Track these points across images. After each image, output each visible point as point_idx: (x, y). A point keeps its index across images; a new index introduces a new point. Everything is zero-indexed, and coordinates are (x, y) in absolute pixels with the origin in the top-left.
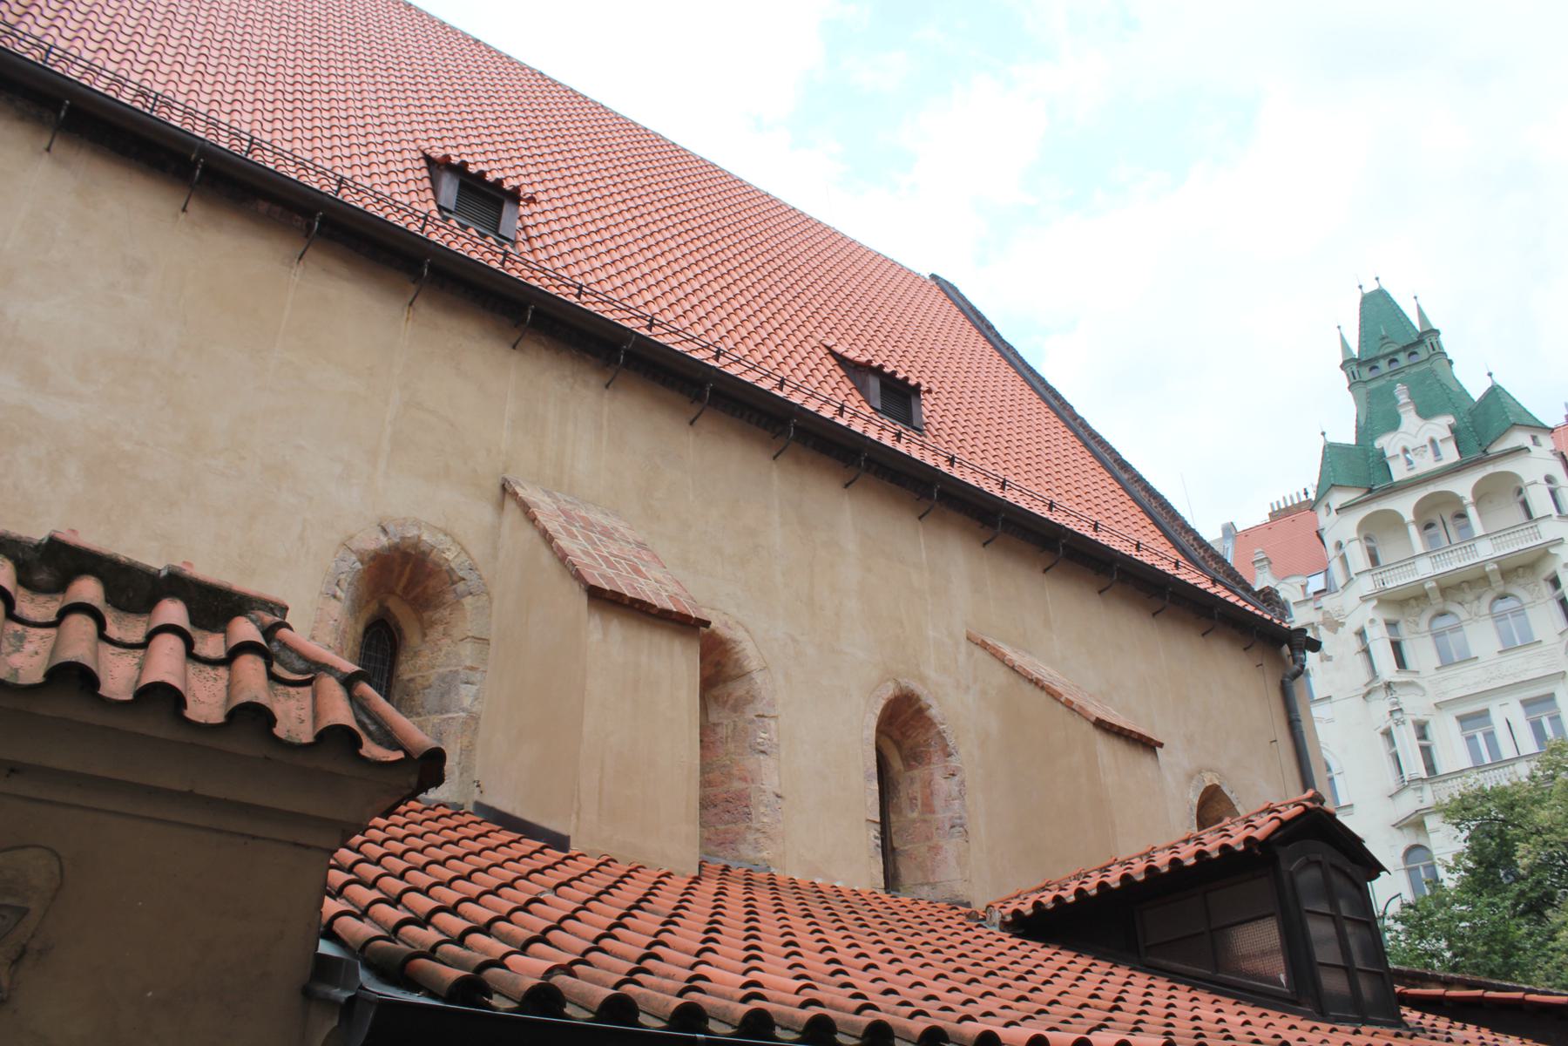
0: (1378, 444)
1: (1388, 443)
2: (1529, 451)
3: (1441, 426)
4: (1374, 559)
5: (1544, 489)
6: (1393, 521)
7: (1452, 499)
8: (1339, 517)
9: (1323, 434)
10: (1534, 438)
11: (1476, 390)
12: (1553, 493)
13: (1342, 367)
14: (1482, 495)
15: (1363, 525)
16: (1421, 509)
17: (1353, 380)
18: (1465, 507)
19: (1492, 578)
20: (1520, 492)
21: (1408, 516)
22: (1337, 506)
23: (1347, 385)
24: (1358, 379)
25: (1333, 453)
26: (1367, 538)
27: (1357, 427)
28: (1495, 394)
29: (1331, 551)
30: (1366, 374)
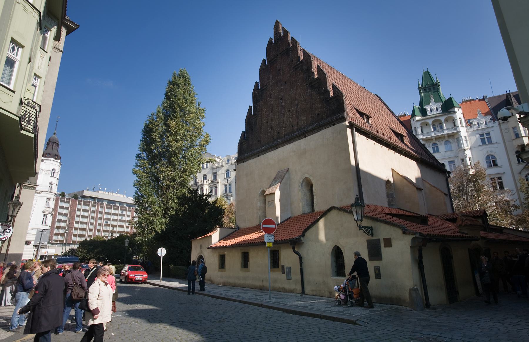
1: (428, 108)
2: (457, 112)
3: (439, 105)
4: (422, 132)
5: (459, 120)
6: (427, 125)
7: (440, 120)
10: (458, 109)
11: (447, 98)
12: (460, 121)
14: (446, 120)
15: (421, 124)
16: (433, 122)
18: (442, 123)
19: (446, 137)
20: (454, 120)
26: (421, 127)
27: (420, 102)
28: (450, 99)
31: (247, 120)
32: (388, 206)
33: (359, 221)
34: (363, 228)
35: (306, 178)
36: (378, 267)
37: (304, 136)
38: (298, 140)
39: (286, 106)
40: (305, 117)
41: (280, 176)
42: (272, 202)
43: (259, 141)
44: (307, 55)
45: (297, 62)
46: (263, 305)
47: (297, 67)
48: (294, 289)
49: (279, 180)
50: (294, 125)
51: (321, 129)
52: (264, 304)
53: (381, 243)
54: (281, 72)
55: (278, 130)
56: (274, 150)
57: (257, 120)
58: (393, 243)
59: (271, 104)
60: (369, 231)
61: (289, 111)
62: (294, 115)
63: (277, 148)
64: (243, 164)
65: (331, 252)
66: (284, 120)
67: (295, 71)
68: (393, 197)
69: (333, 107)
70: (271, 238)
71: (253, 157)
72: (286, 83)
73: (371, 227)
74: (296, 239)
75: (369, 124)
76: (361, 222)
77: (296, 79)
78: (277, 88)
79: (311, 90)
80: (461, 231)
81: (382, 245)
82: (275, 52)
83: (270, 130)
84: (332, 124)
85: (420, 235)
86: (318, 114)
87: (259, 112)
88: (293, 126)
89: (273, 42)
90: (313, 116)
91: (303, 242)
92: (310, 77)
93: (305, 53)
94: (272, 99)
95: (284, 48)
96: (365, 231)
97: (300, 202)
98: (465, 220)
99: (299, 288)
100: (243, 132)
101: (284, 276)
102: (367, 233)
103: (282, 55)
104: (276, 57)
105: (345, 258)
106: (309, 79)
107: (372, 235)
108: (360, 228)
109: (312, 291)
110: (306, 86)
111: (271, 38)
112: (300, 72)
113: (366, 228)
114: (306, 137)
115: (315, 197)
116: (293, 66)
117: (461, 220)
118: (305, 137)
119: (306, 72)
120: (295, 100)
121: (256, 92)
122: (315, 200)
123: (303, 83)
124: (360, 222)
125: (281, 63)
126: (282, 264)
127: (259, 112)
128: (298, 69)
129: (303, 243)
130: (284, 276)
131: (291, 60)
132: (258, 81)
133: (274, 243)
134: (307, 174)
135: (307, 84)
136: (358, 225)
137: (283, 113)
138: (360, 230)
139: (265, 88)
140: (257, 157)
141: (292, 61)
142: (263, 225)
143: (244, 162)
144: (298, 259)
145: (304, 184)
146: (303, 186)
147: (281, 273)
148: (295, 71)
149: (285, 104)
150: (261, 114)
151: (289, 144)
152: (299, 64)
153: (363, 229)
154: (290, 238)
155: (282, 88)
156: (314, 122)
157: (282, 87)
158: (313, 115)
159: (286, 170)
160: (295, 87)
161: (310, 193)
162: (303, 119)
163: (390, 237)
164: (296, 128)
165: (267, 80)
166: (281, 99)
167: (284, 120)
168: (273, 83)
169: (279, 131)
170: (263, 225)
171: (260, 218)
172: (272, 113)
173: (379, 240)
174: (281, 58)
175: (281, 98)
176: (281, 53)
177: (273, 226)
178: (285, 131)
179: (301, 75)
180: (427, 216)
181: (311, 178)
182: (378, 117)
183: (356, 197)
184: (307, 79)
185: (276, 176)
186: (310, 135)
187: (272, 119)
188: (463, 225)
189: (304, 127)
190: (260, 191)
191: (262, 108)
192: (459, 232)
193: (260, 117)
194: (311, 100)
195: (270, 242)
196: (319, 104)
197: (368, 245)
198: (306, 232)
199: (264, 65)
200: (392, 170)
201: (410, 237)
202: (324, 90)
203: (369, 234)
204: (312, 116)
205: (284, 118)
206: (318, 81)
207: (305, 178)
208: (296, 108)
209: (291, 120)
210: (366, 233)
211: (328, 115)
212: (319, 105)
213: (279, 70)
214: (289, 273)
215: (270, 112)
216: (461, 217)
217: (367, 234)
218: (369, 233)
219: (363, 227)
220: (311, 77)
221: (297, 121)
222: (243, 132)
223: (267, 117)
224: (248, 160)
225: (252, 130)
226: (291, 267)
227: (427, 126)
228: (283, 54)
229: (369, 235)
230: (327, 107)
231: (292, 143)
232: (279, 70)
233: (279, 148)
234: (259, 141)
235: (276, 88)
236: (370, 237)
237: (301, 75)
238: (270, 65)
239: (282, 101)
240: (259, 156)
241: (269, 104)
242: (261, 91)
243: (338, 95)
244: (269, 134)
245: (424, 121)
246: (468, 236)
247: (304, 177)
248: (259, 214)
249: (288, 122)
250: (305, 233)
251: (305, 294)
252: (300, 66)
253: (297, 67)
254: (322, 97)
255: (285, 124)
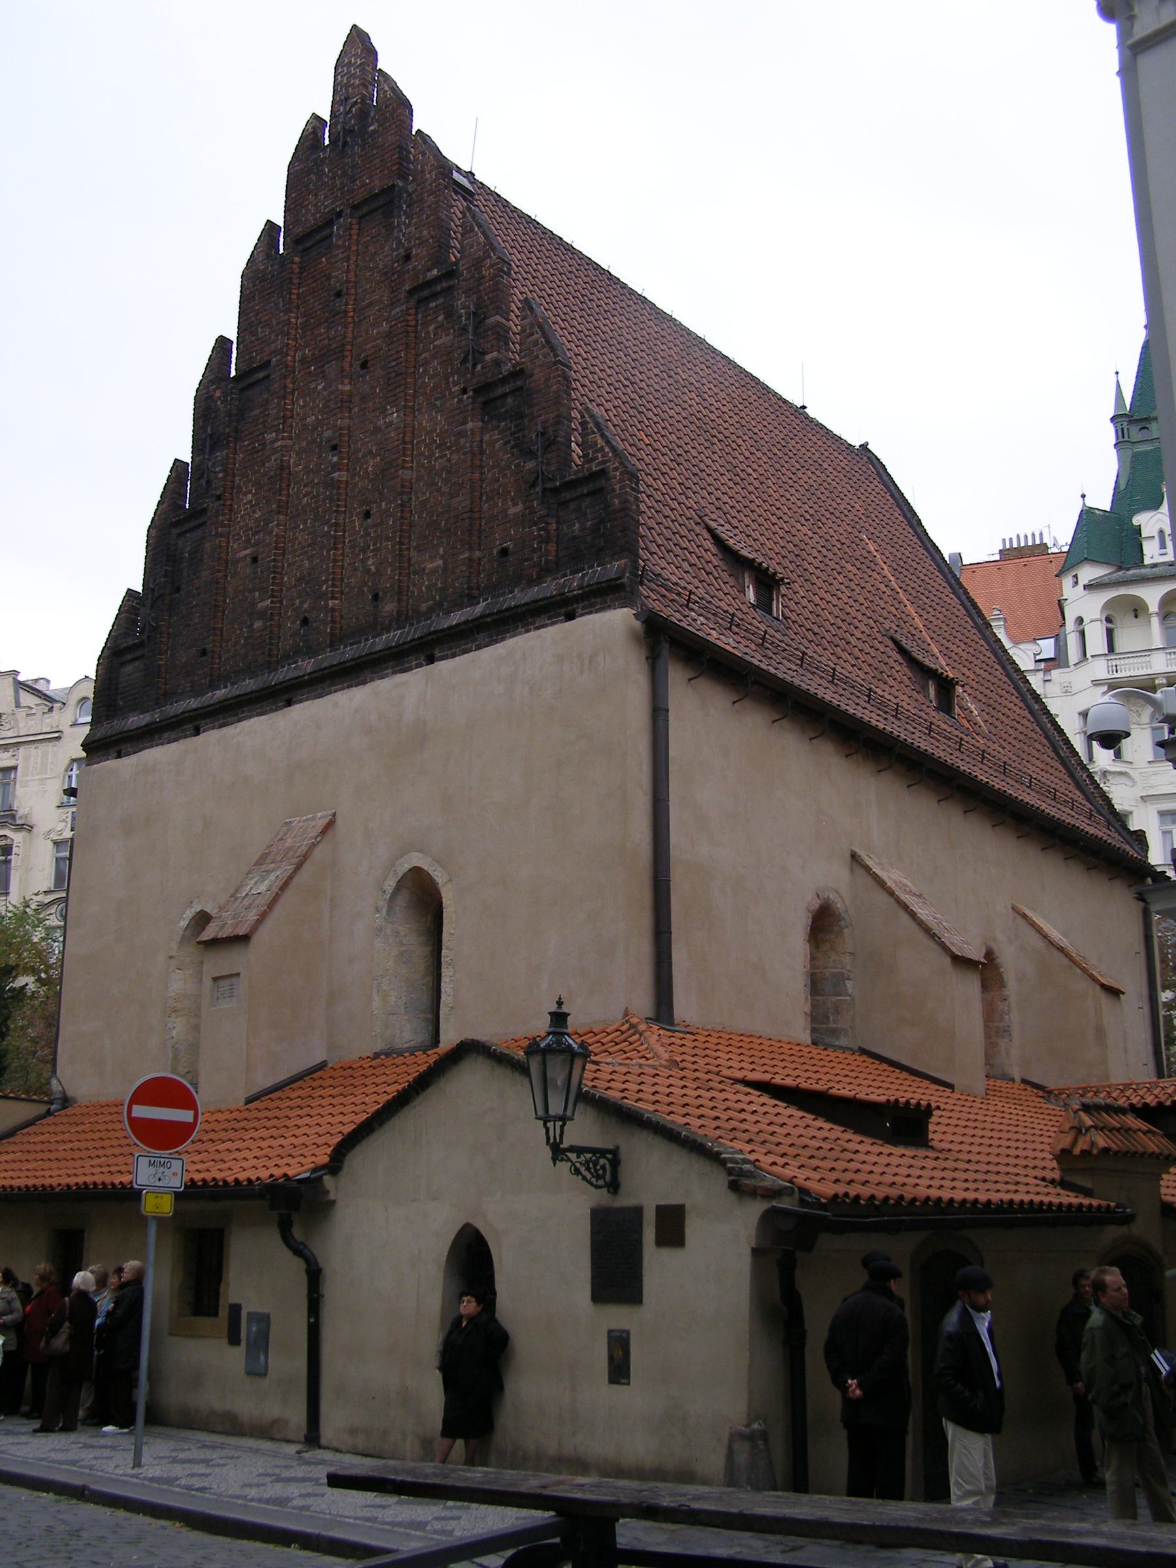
0: (1136, 520)
6: (1137, 609)
8: (1086, 592)
9: (1083, 496)
13: (1112, 419)
15: (1108, 605)
17: (1121, 439)
21: (1153, 607)
22: (1086, 582)
23: (1114, 441)
24: (1126, 439)
25: (1088, 516)
26: (1109, 620)
29: (1070, 625)
30: (1135, 434)
31: (153, 532)
32: (806, 1038)
33: (555, 1122)
34: (573, 1156)
35: (417, 871)
36: (624, 1335)
37: (423, 658)
38: (395, 673)
39: (356, 485)
40: (442, 557)
41: (289, 849)
42: (234, 980)
43: (204, 653)
44: (482, 239)
45: (429, 270)
46: (89, 1490)
47: (426, 293)
48: (275, 1422)
49: (279, 867)
50: (381, 594)
51: (508, 632)
52: (93, 1487)
53: (645, 1224)
54: (347, 304)
55: (305, 606)
56: (272, 711)
57: (204, 538)
58: (693, 1228)
59: (282, 468)
60: (603, 1167)
61: (367, 515)
62: (388, 539)
63: (289, 703)
64: (111, 764)
65: (446, 1254)
66: (335, 561)
67: (417, 308)
68: (840, 995)
69: (577, 526)
70: (169, 1172)
71: (166, 735)
72: (364, 365)
73: (615, 1152)
74: (299, 1181)
75: (770, 613)
76: (562, 1127)
77: (417, 355)
78: (320, 387)
79: (480, 423)
80: (1067, 1178)
81: (649, 1234)
82: (326, 197)
83: (261, 605)
84: (563, 611)
85: (802, 1202)
86: (504, 552)
87: (219, 498)
88: (376, 597)
89: (327, 142)
90: (479, 559)
91: (332, 1196)
92: (484, 353)
93: (472, 229)
94: (289, 443)
95: (377, 182)
96: (582, 1169)
97: (374, 994)
98: (1088, 1129)
99: (297, 1416)
100: (130, 593)
101: (237, 1355)
102: (589, 1176)
103: (361, 218)
104: (330, 223)
105: (498, 1287)
106: (479, 367)
107: (614, 1186)
108: (558, 1152)
109: (353, 1431)
110: (460, 401)
111: (315, 117)
112: (440, 318)
113: (589, 1156)
114: (432, 663)
115: (446, 973)
116: (407, 287)
117: (1072, 1128)
118: (431, 660)
119: (464, 329)
120: (400, 462)
121: (215, 390)
122: (446, 986)
123: (448, 383)
124: (559, 1124)
125: (353, 258)
126: (233, 1299)
127: (219, 498)
128: (433, 305)
129: (333, 1202)
130: (237, 1355)
131: (401, 251)
132: (232, 335)
133: (178, 1196)
134: (421, 851)
135: (464, 391)
136: (552, 1140)
137: (336, 524)
138: (554, 1160)
139: (261, 375)
140: (186, 737)
141: (408, 257)
142: (134, 1107)
143: (119, 756)
144: (303, 1279)
145: (401, 901)
146: (397, 909)
147: (226, 1341)
148: (417, 308)
149: (353, 476)
150: (231, 511)
151: (349, 687)
152: (437, 280)
153: (569, 1160)
154: (271, 1176)
155: (342, 393)
156: (478, 589)
157: (342, 383)
158: (477, 554)
159: (326, 820)
160: (406, 394)
161: (429, 948)
162: (430, 566)
163: (680, 1202)
164: (389, 607)
165: (277, 336)
166: (334, 448)
167: (335, 561)
168: (303, 360)
169: (306, 614)
170: (134, 1107)
171: (175, 1058)
172: (282, 517)
173: (638, 1211)
174: (354, 232)
175: (335, 442)
176: (355, 208)
177: (186, 1116)
178: (338, 619)
179: (444, 340)
180: (929, 1105)
181: (439, 876)
182: (840, 578)
183: (553, 1008)
184: (470, 365)
185: (269, 847)
186: (454, 656)
187: (276, 548)
188: (1077, 1151)
189: (431, 610)
190: (189, 914)
191: (237, 478)
192: (1063, 1184)
193: (223, 526)
194: (477, 475)
195: (158, 1192)
196: (512, 500)
197: (594, 1233)
198: (348, 1151)
199: (268, 256)
200: (854, 856)
201: (757, 1208)
202: (543, 434)
203: (601, 1182)
204: (470, 559)
205: (336, 549)
206: (519, 383)
207: (410, 870)
208: (402, 505)
209: (371, 562)
210: (584, 1178)
211: (547, 561)
212: (515, 505)
213: (339, 294)
214: (260, 1343)
215: (274, 506)
216: (1075, 1112)
217: (591, 1183)
218: (598, 1177)
219: (572, 1149)
220: (488, 357)
221: (397, 572)
222: (130, 593)
223: (257, 533)
224: (144, 749)
225: (178, 590)
226: (268, 1316)
227: (1136, 617)
228: (369, 213)
229: (597, 1187)
230: (550, 520)
231: (364, 683)
232: (339, 294)
233: (301, 701)
234: (204, 653)
235: (313, 385)
236: (601, 1197)
237: (444, 340)
238: (297, 259)
239: (335, 459)
240: (197, 732)
241: (273, 461)
242: (242, 390)
243: (603, 473)
244: (258, 624)
245: (1123, 591)
246: (1095, 1203)
247: (407, 867)
248: (174, 1033)
249: (356, 569)
250: (344, 1155)
251: (320, 1447)
252: (442, 291)
253: (426, 293)
254: (530, 465)
255: (342, 580)
